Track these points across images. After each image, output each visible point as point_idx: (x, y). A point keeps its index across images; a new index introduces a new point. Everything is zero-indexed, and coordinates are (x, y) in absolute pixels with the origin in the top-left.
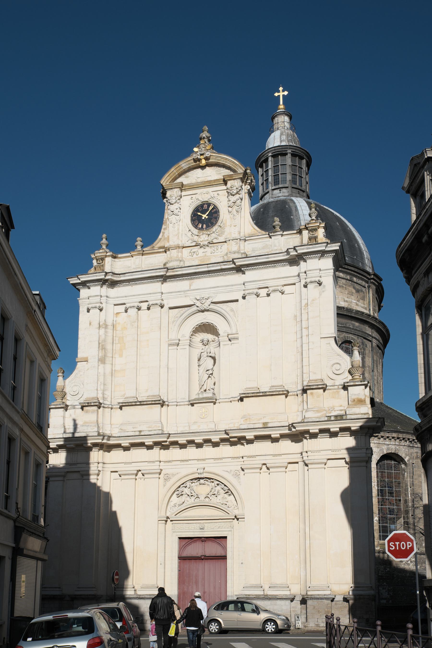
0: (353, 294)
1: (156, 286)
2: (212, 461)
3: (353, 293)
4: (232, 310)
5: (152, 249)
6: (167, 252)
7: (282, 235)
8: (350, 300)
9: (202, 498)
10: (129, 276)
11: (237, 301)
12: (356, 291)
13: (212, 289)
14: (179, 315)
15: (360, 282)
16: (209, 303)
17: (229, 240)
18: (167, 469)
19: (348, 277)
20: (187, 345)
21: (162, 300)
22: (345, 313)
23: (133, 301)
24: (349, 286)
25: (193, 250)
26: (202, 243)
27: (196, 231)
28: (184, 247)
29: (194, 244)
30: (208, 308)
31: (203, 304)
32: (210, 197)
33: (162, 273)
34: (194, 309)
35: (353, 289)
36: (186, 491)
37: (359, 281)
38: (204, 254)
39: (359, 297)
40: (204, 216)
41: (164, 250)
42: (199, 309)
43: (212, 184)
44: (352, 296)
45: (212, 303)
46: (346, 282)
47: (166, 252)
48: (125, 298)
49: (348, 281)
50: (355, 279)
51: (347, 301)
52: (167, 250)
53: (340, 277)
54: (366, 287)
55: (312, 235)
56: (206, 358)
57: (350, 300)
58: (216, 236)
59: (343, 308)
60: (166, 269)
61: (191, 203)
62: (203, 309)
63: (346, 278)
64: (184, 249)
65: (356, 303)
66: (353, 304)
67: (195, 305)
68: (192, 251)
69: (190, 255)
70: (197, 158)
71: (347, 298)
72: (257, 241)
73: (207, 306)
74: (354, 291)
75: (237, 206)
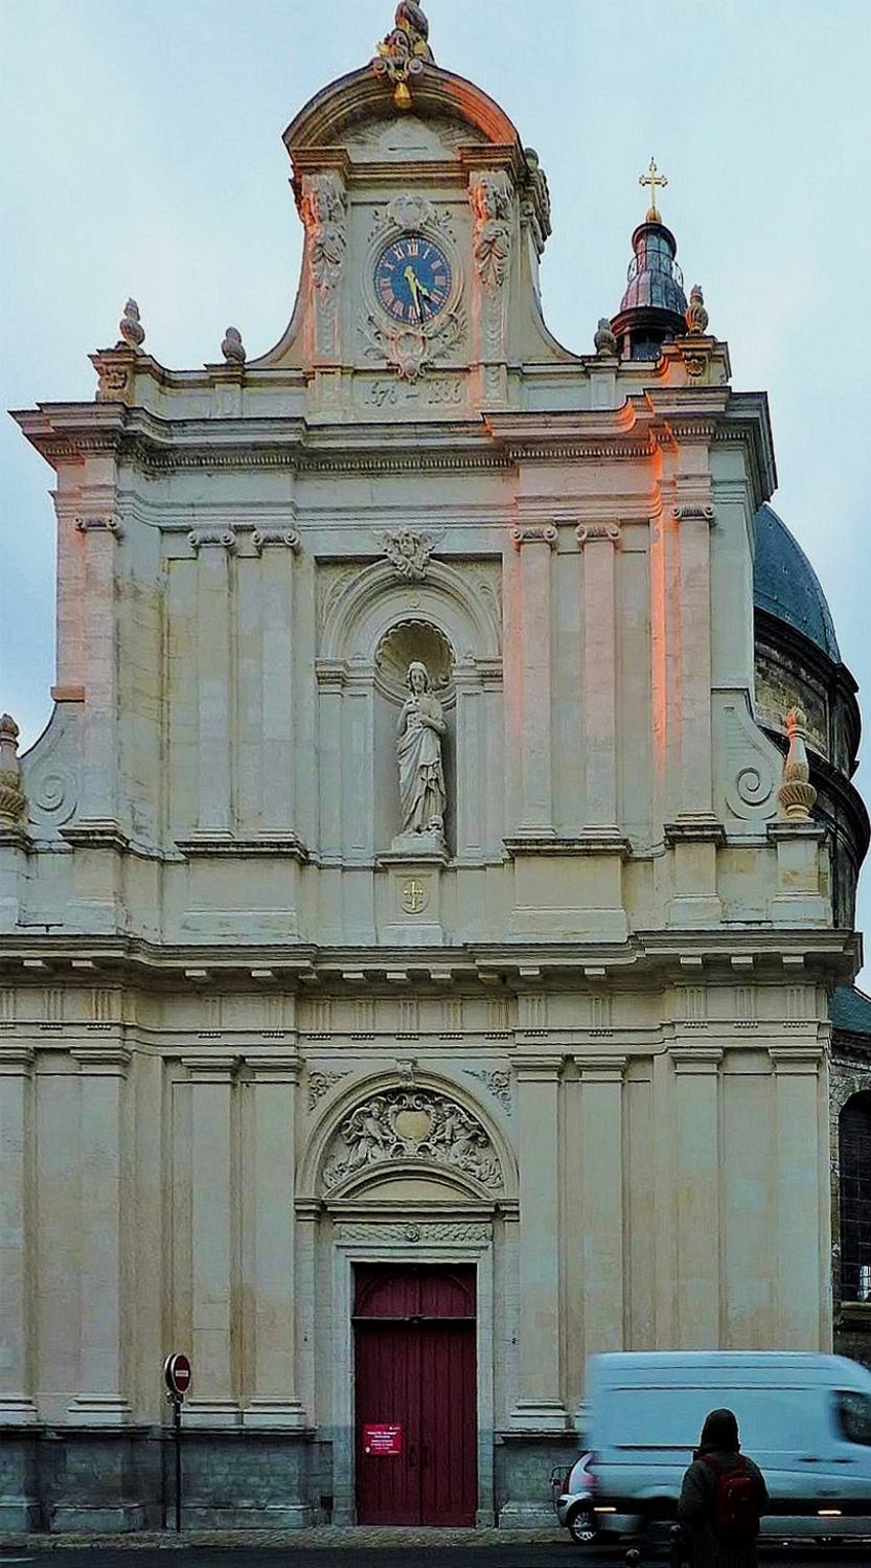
1: (278, 485)
2: (435, 1041)
9: (411, 1150)
13: (431, 514)
18: (319, 1058)
23: (216, 523)
25: (382, 387)
27: (386, 324)
28: (356, 372)
34: (382, 572)
36: (370, 1124)
42: (397, 573)
48: (191, 511)
61: (374, 230)
64: (357, 378)
67: (386, 557)
68: (378, 390)
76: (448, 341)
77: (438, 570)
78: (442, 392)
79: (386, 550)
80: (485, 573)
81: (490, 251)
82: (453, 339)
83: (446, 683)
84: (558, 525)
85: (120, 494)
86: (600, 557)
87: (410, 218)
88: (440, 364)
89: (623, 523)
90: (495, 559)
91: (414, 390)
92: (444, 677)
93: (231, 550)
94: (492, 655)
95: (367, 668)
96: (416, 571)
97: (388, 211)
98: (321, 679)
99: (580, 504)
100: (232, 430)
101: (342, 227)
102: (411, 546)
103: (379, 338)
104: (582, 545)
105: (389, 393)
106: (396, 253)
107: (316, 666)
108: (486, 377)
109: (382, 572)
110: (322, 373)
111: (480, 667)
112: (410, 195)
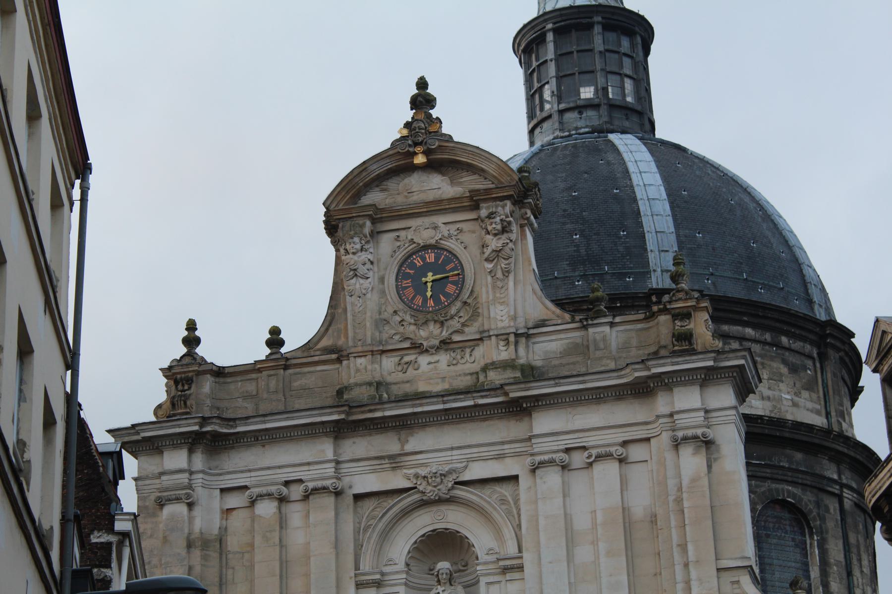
0: (783, 378)
3: (781, 375)
4: (503, 501)
5: (306, 354)
6: (345, 363)
7: (612, 325)
8: (777, 393)
10: (256, 423)
11: (514, 479)
12: (789, 369)
13: (455, 452)
14: (379, 512)
15: (797, 345)
16: (450, 485)
17: (490, 336)
19: (768, 337)
20: (400, 584)
21: (339, 479)
22: (766, 431)
24: (772, 359)
25: (407, 359)
26: (425, 344)
29: (407, 345)
31: (435, 487)
32: (440, 237)
33: (335, 417)
35: (782, 366)
37: (794, 343)
38: (431, 366)
39: (798, 385)
40: (430, 277)
41: (334, 356)
42: (425, 498)
43: (443, 207)
44: (781, 385)
45: (456, 483)
46: (763, 349)
47: (339, 360)
49: (767, 347)
50: (784, 340)
51: (769, 398)
52: (342, 356)
53: (747, 337)
54: (815, 355)
55: (681, 326)
57: (777, 393)
58: (458, 326)
59: (761, 417)
60: (346, 408)
62: (437, 498)
63: (762, 339)
65: (792, 400)
66: (785, 402)
67: (415, 488)
68: (403, 361)
69: (400, 368)
70: (408, 150)
71: (769, 388)
72: (553, 337)
73: (444, 490)
74: (784, 370)
75: (504, 259)
76: (462, 320)
77: (461, 493)
78: (459, 357)
79: (416, 483)
80: (505, 490)
81: (498, 255)
82: (466, 318)
83: (465, 568)
84: (568, 450)
85: (191, 473)
86: (608, 471)
87: (426, 236)
88: (456, 338)
89: (625, 444)
90: (515, 478)
91: (435, 358)
92: (463, 564)
93: (282, 500)
94: (511, 549)
95: (397, 573)
96: (441, 495)
97: (410, 235)
98: (359, 585)
99: (587, 434)
100: (288, 418)
101: (371, 253)
103: (403, 325)
104: (590, 464)
105: (413, 362)
106: (416, 262)
107: (355, 577)
108: (498, 344)
109: (416, 497)
110: (355, 357)
111: (502, 563)
112: (427, 221)
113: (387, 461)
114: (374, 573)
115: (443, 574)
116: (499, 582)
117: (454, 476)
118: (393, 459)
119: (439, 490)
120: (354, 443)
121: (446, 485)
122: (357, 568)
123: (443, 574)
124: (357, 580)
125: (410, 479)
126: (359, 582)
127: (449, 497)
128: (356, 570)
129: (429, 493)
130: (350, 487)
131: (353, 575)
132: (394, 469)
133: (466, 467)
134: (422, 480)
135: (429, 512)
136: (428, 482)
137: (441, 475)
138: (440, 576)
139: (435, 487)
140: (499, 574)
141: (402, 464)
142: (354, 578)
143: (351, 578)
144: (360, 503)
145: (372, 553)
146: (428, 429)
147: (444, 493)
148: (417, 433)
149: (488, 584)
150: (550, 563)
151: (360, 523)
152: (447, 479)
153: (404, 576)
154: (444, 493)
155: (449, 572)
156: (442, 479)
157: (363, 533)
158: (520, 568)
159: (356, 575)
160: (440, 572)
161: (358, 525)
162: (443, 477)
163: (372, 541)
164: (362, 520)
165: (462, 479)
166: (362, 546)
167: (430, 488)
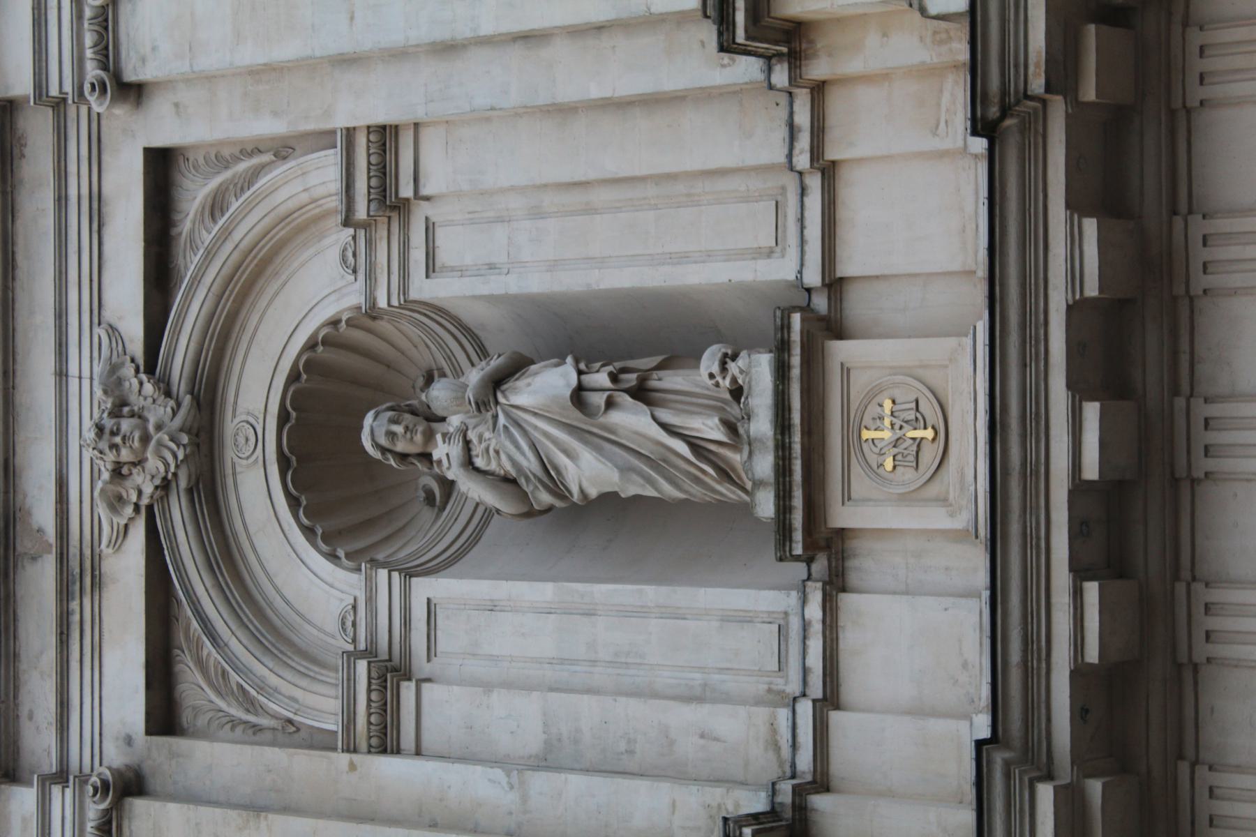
16: (149, 388)
30: (187, 400)
31: (145, 439)
45: (150, 368)
56: (502, 420)
62: (185, 439)
67: (150, 508)
73: (158, 412)
96: (178, 421)
102: (126, 425)
107: (355, 751)
109: (178, 511)
111: (361, 213)
113: (75, 605)
114: (351, 681)
115: (391, 435)
116: (430, 228)
117: (129, 370)
118: (74, 583)
119: (159, 427)
120: (31, 717)
121: (150, 400)
122: (320, 742)
123: (391, 435)
124: (363, 745)
125: (126, 526)
126: (374, 741)
127: (188, 397)
128: (334, 749)
129: (167, 465)
130: (129, 740)
131: (343, 759)
132: (98, 583)
133: (113, 330)
134: (128, 483)
135: (234, 474)
136: (134, 464)
137: (116, 413)
138: (401, 447)
139: (145, 439)
140: (405, 226)
141: (87, 552)
142: (355, 757)
143: (352, 767)
144: (186, 717)
145: (304, 682)
146: (20, 459)
147: (174, 413)
148: (25, 496)
149: (431, 268)
150: (352, 18)
151: (234, 723)
152: (133, 398)
153: (383, 574)
154: (174, 413)
155: (390, 414)
156: (132, 415)
157: (256, 714)
158: (385, 136)
159: (351, 748)
160: (383, 441)
161: (239, 730)
162: (126, 410)
163: (273, 680)
164: (228, 715)
165: (136, 346)
166: (290, 721)
167: (153, 463)
